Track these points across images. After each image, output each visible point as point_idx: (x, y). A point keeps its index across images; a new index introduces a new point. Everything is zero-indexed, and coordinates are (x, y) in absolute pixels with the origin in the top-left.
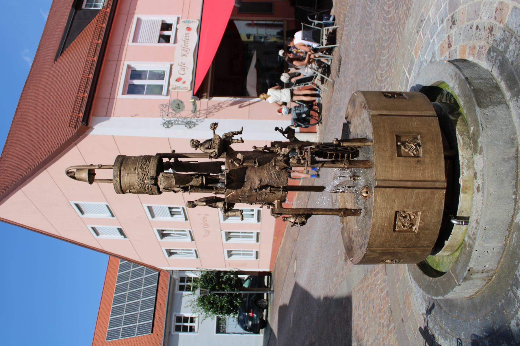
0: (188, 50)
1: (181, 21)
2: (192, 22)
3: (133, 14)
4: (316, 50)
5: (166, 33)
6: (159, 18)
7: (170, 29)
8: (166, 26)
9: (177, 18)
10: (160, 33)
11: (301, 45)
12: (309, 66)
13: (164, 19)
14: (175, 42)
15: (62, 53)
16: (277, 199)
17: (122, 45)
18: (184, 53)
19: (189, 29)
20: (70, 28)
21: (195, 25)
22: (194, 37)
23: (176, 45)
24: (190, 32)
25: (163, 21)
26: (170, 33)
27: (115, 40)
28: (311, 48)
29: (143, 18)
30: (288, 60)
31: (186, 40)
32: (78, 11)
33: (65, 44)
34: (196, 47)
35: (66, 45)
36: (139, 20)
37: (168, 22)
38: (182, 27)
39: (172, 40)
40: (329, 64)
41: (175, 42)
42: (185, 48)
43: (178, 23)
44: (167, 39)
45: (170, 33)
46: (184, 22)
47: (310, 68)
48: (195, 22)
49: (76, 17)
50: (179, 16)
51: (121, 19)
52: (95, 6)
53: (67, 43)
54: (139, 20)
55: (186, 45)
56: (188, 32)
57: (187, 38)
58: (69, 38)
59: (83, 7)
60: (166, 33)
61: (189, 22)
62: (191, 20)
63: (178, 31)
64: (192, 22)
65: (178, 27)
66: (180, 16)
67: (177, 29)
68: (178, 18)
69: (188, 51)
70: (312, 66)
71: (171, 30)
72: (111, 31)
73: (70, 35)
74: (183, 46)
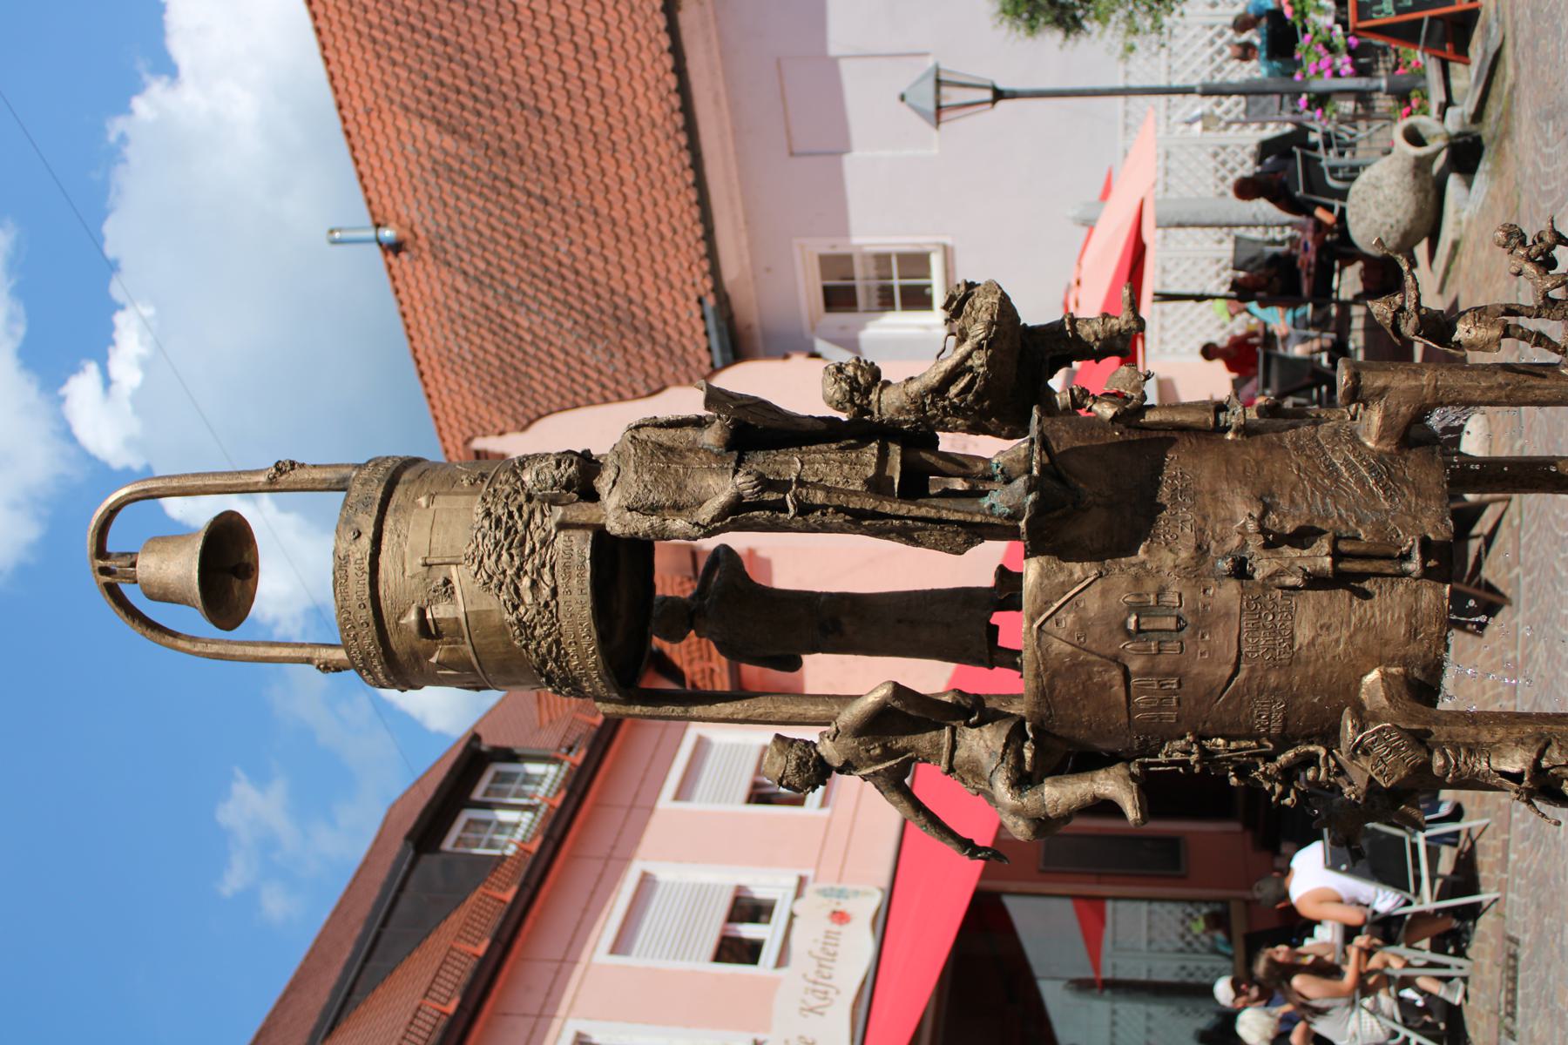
0: (832, 992)
1: (809, 889)
2: (857, 893)
3: (627, 860)
4: (1388, 929)
5: (748, 931)
6: (723, 879)
7: (763, 918)
8: (748, 909)
9: (794, 882)
10: (724, 930)
11: (1321, 902)
12: (1367, 1002)
13: (744, 880)
14: (782, 961)
15: (332, 1029)
16: (1380, 661)
17: (567, 961)
18: (813, 1001)
19: (840, 917)
20: (384, 924)
21: (865, 905)
22: (859, 948)
23: (783, 972)
24: (845, 929)
25: (739, 888)
26: (765, 933)
27: (542, 942)
28: (1369, 912)
29: (665, 873)
30: (1268, 971)
31: (827, 955)
32: (426, 859)
33: (349, 994)
34: (864, 983)
35: (355, 997)
36: (646, 881)
37: (760, 893)
38: (813, 912)
39: (769, 955)
40: (1457, 999)
41: (782, 961)
42: (820, 986)
43: (799, 894)
44: (748, 952)
45: (765, 933)
46: (824, 893)
47: (1372, 1013)
48: (866, 894)
49: (412, 881)
50: (804, 872)
51: (573, 878)
52: (491, 845)
53: (358, 988)
54: (646, 881)
55: (826, 972)
56: (835, 928)
57: (831, 949)
58: (372, 964)
59: (448, 845)
60: (748, 931)
61: (841, 894)
62: (850, 887)
63: (796, 921)
64: (857, 893)
65: (797, 910)
66: (809, 872)
67: (792, 916)
68: (802, 881)
69: (832, 994)
70: (1376, 1001)
71: (768, 922)
72: (534, 911)
73: (377, 954)
74: (812, 976)
